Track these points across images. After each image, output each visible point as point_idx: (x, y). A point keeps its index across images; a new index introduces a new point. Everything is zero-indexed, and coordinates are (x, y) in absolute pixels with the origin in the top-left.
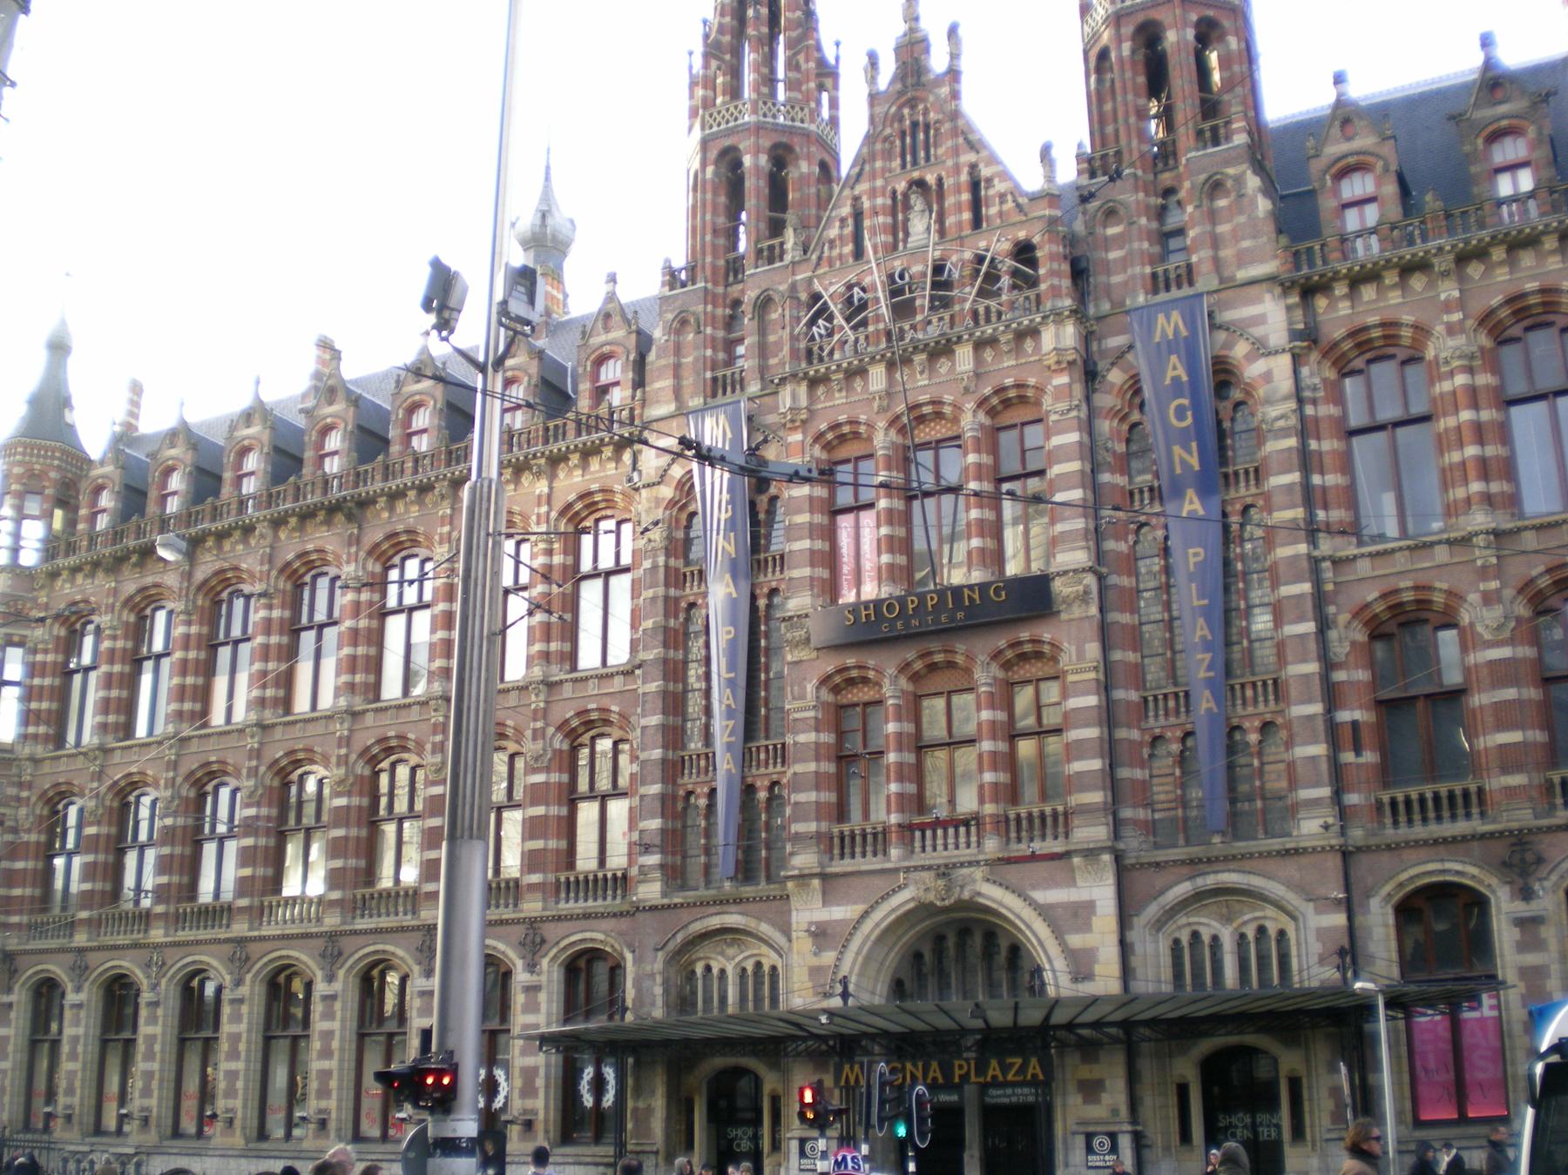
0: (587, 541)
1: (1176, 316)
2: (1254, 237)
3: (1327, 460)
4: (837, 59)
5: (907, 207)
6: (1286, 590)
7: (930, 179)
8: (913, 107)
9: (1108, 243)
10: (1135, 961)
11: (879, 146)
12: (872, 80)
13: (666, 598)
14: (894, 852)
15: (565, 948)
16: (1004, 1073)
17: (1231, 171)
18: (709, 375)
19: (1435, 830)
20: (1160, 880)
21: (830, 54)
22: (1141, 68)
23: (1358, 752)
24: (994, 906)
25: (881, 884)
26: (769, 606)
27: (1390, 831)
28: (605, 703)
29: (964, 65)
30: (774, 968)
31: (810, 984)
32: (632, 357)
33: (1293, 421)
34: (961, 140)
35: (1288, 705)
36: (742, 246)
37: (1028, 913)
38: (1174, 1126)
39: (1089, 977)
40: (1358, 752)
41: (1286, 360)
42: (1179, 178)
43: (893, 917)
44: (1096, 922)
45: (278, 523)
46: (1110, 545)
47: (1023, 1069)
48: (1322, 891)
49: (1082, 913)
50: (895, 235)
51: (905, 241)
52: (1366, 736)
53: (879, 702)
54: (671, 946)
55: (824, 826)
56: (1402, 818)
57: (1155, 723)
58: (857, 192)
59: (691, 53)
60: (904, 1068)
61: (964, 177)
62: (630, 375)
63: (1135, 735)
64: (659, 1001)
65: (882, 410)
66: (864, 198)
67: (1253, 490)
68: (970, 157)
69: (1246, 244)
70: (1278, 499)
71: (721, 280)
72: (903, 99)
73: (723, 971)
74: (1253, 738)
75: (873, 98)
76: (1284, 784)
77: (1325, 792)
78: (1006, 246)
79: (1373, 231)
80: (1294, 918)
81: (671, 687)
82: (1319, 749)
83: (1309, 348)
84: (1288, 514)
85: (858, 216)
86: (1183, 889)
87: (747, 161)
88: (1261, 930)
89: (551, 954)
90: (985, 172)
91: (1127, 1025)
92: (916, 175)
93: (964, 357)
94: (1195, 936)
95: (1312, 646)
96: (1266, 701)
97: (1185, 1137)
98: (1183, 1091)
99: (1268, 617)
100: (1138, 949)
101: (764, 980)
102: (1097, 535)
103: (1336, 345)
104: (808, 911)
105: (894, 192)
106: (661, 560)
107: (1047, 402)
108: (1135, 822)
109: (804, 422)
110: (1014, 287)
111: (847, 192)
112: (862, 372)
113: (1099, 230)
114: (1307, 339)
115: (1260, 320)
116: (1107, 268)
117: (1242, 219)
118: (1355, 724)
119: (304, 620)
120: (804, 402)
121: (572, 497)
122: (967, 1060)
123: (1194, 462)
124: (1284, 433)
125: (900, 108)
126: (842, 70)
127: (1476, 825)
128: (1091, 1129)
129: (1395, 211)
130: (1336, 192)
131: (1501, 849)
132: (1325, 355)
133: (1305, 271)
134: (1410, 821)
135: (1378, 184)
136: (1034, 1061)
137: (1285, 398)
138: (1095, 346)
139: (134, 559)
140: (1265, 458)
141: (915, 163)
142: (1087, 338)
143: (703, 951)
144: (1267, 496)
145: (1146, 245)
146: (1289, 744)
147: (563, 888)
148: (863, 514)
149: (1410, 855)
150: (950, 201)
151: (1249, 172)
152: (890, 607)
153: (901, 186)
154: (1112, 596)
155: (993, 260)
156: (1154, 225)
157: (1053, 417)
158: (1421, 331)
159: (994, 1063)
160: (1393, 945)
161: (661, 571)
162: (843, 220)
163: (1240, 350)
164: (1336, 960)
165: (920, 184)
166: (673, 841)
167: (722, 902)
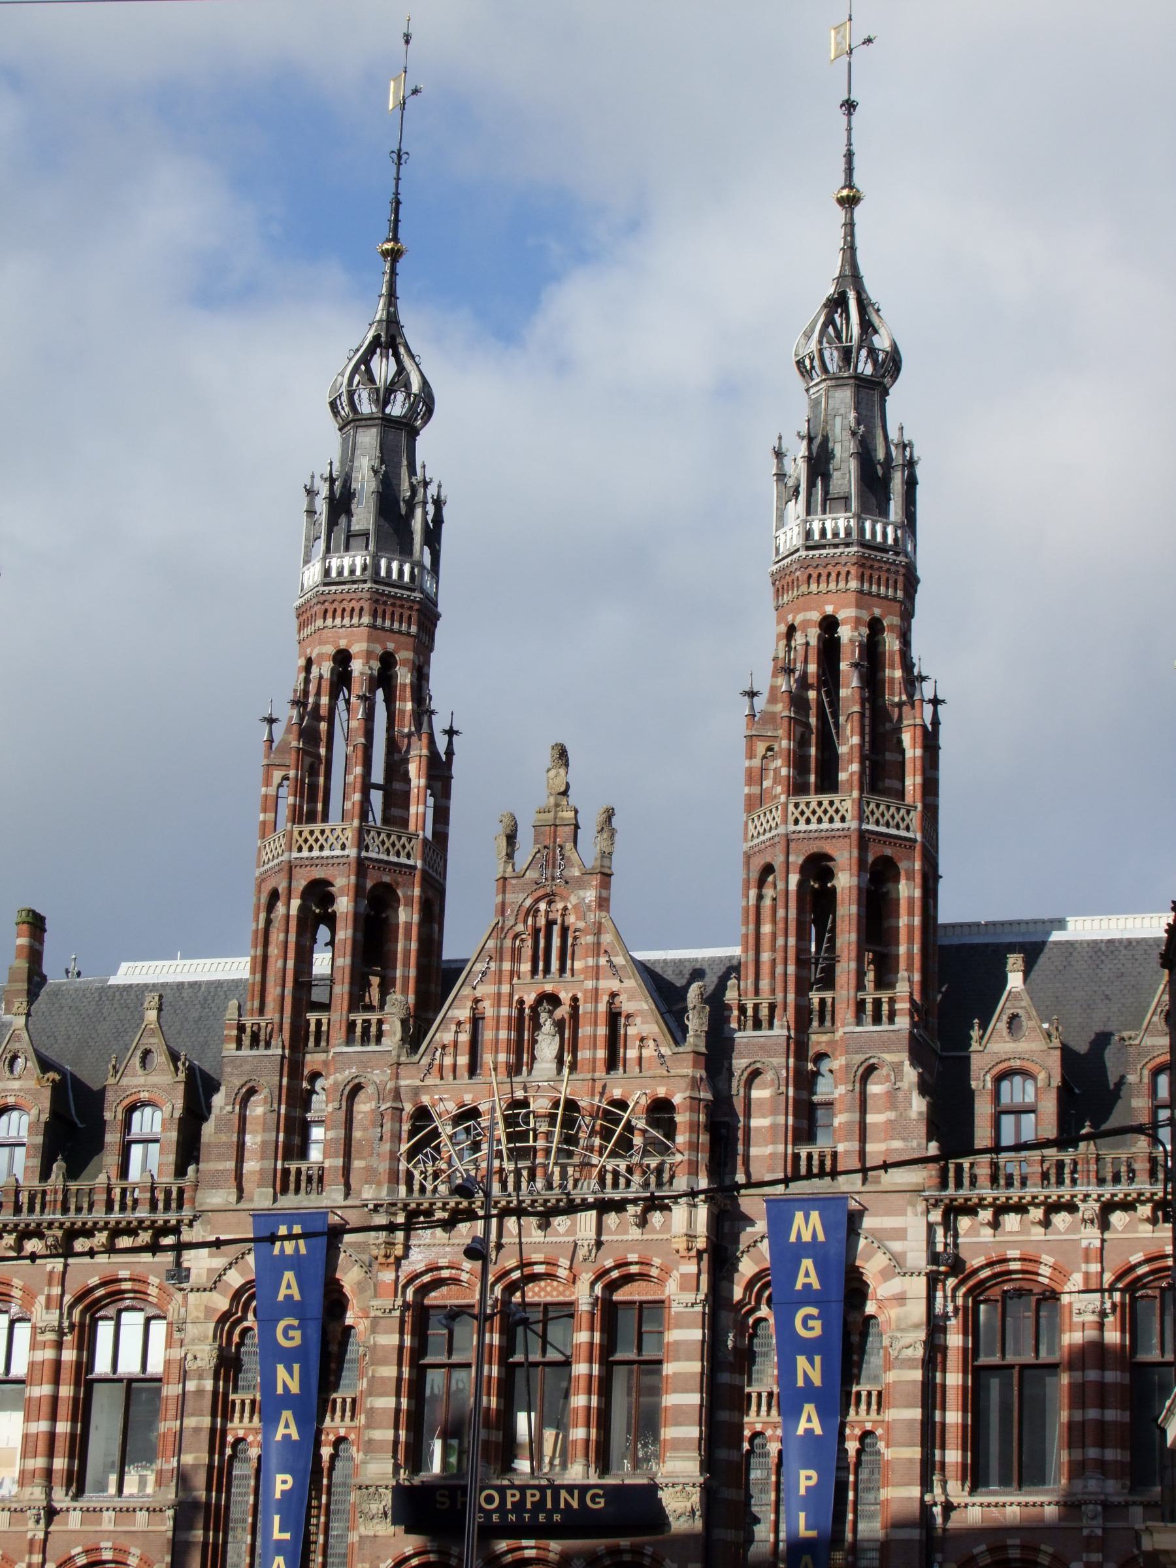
0: (105, 1331)
1: (815, 1216)
2: (904, 1139)
4: (450, 752)
5: (537, 1026)
7: (565, 996)
8: (550, 903)
17: (888, 1057)
21: (441, 743)
26: (334, 1457)
34: (603, 961)
41: (921, 1284)
58: (478, 993)
59: (271, 721)
61: (602, 1007)
62: (174, 1135)
66: (486, 1004)
68: (613, 985)
72: (541, 893)
78: (644, 1101)
85: (476, 1021)
92: (549, 988)
105: (521, 1002)
115: (900, 1234)
121: (94, 1281)
125: (537, 901)
137: (916, 1326)
138: (727, 1225)
144: (888, 1426)
151: (907, 1063)
153: (530, 999)
155: (629, 1121)
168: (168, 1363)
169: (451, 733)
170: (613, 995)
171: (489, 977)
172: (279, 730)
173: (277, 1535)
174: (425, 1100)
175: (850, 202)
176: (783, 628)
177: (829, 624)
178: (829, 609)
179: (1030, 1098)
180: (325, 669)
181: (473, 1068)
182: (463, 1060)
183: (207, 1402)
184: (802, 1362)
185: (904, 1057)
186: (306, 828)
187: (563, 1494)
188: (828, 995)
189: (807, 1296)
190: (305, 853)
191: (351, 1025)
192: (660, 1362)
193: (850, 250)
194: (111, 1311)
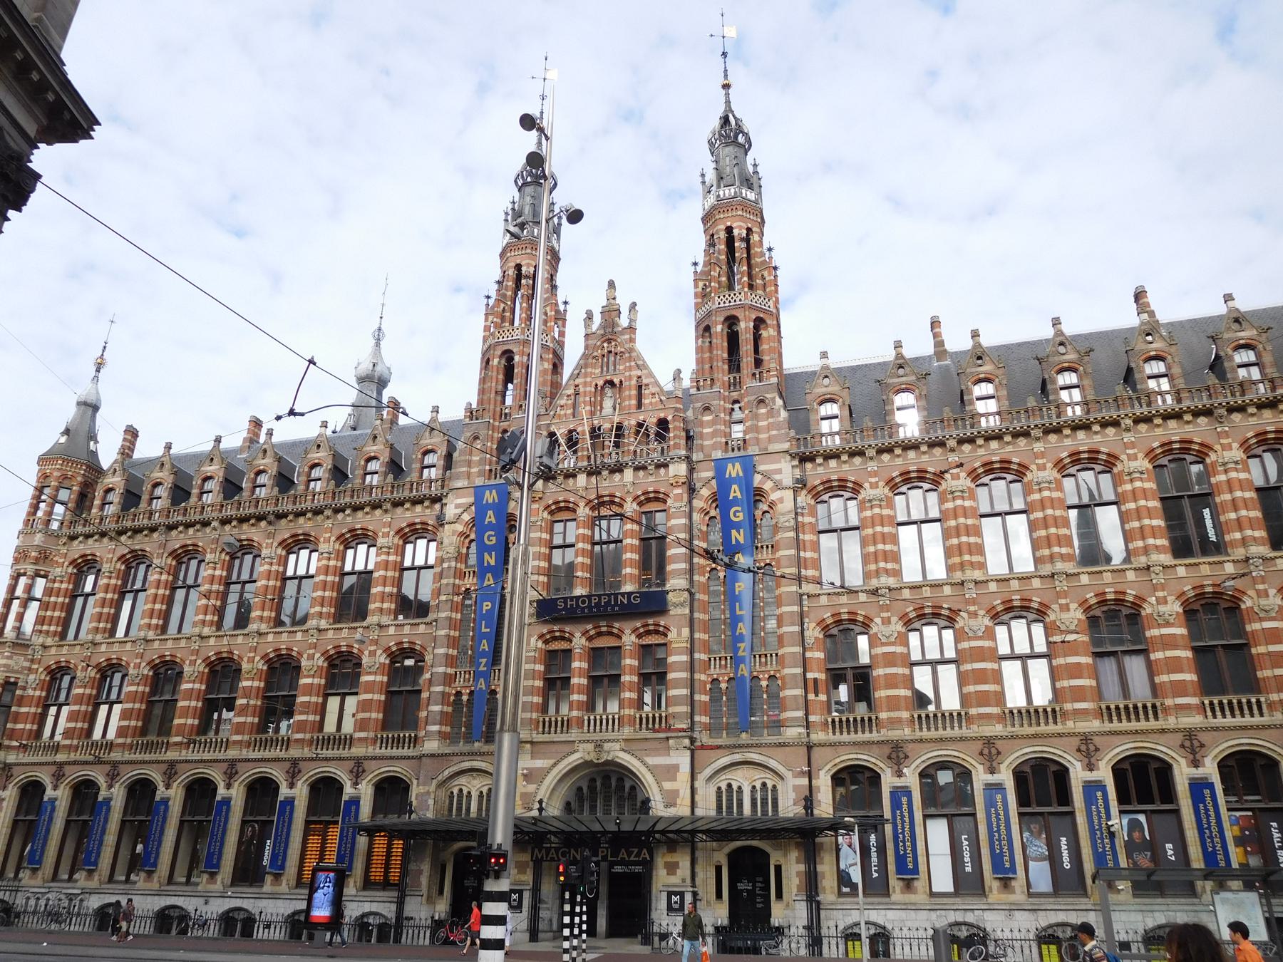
0: (409, 547)
1: (737, 465)
3: (808, 545)
5: (603, 394)
6: (785, 609)
7: (616, 381)
9: (702, 424)
10: (697, 798)
12: (587, 326)
14: (574, 730)
15: (377, 775)
16: (629, 857)
17: (768, 396)
18: (487, 468)
19: (853, 737)
21: (562, 307)
22: (725, 338)
23: (817, 695)
24: (626, 764)
25: (566, 748)
33: (792, 523)
34: (633, 363)
36: (509, 400)
39: (674, 805)
40: (817, 695)
42: (742, 396)
43: (570, 767)
44: (679, 776)
45: (225, 522)
47: (638, 855)
49: (672, 771)
51: (601, 411)
52: (822, 687)
53: (570, 651)
55: (534, 715)
56: (837, 730)
58: (577, 381)
60: (569, 852)
61: (634, 382)
62: (442, 462)
63: (703, 677)
67: (770, 556)
68: (639, 373)
70: (783, 562)
71: (498, 418)
74: (764, 683)
75: (587, 336)
77: (800, 714)
78: (655, 420)
79: (837, 433)
82: (799, 692)
83: (802, 488)
87: (517, 358)
88: (764, 784)
89: (369, 778)
90: (645, 381)
91: (693, 833)
92: (608, 378)
93: (628, 474)
94: (729, 786)
96: (771, 664)
97: (719, 895)
98: (718, 870)
99: (774, 622)
102: (691, 571)
106: (453, 564)
107: (670, 502)
109: (540, 498)
111: (572, 382)
112: (574, 476)
115: (779, 471)
116: (702, 436)
118: (815, 680)
119: (234, 578)
122: (607, 848)
124: (788, 529)
127: (874, 736)
128: (670, 889)
129: (847, 426)
133: (802, 449)
134: (841, 733)
139: (129, 534)
142: (691, 470)
144: (778, 561)
146: (783, 688)
147: (379, 741)
148: (567, 550)
149: (840, 749)
153: (601, 383)
154: (696, 604)
157: (673, 510)
159: (623, 850)
163: (767, 486)
164: (803, 803)
165: (611, 383)
167: (473, 755)
169: (566, 303)
170: (639, 377)
172: (491, 302)
173: (484, 630)
175: (726, 87)
177: (729, 230)
178: (729, 224)
180: (511, 272)
183: (452, 571)
184: (734, 532)
187: (620, 597)
188: (737, 376)
193: (728, 102)
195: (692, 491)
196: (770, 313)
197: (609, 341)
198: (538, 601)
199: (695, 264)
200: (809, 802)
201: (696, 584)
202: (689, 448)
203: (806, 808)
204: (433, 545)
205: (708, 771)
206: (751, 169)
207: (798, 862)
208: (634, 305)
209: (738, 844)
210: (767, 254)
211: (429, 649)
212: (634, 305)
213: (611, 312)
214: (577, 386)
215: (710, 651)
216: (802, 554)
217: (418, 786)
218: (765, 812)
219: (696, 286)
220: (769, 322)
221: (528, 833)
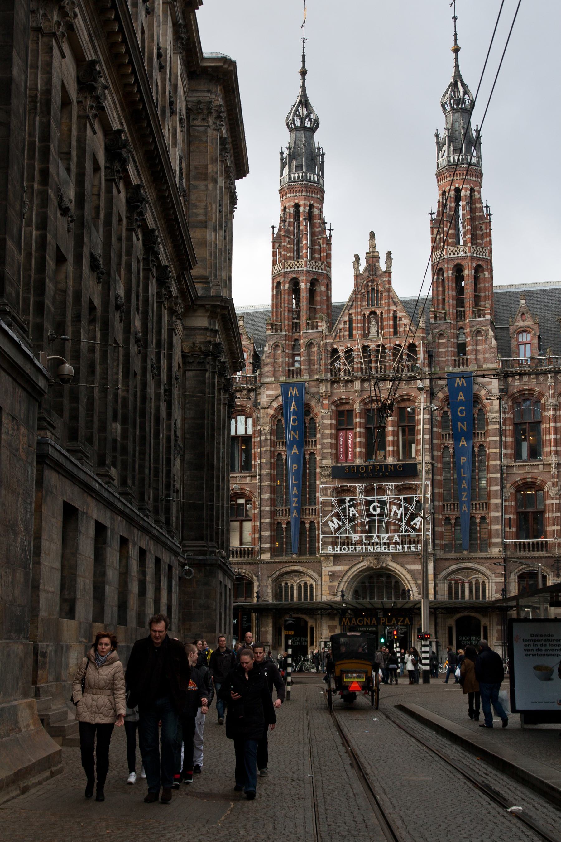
0: (233, 422)
3: (507, 433)
4: (330, 236)
5: (369, 322)
6: (492, 475)
7: (378, 312)
9: (440, 345)
10: (437, 589)
11: (359, 296)
12: (357, 269)
13: (271, 451)
17: (484, 328)
18: (287, 368)
20: (447, 563)
21: (328, 233)
23: (510, 528)
27: (518, 553)
28: (244, 486)
29: (393, 269)
30: (311, 585)
31: (328, 592)
32: (252, 353)
34: (391, 300)
35: (490, 512)
37: (404, 572)
38: (447, 640)
40: (510, 528)
46: (435, 453)
47: (403, 621)
48: (497, 571)
50: (364, 330)
52: (513, 523)
54: (274, 576)
56: (522, 549)
57: (447, 513)
59: (273, 227)
61: (391, 315)
63: (440, 516)
64: (270, 595)
65: (358, 396)
66: (353, 315)
67: (483, 440)
69: (487, 355)
70: (491, 445)
73: (292, 585)
74: (478, 521)
76: (487, 536)
80: (488, 578)
81: (273, 484)
84: (494, 451)
85: (351, 321)
86: (454, 567)
92: (373, 310)
95: (499, 494)
98: (450, 629)
99: (485, 482)
100: (439, 585)
101: (306, 589)
102: (432, 450)
103: (513, 394)
104: (328, 568)
105: (364, 314)
106: (269, 437)
108: (439, 544)
110: (409, 361)
111: (347, 311)
112: (352, 381)
113: (437, 341)
114: (505, 392)
117: (486, 346)
118: (510, 519)
120: (329, 390)
123: (465, 428)
124: (495, 423)
125: (368, 282)
126: (333, 241)
130: (517, 339)
131: (551, 561)
132: (509, 397)
134: (525, 551)
135: (532, 339)
136: (407, 619)
137: (496, 412)
140: (489, 430)
141: (372, 305)
143: (286, 577)
144: (488, 443)
145: (453, 349)
146: (490, 524)
150: (386, 323)
152: (362, 469)
153: (367, 313)
154: (435, 470)
156: (456, 341)
158: (541, 394)
160: (517, 588)
161: (269, 441)
162: (345, 322)
163: (483, 393)
165: (374, 313)
166: (272, 539)
167: (295, 563)
168: (254, 431)
169: (330, 230)
170: (395, 311)
171: (353, 307)
172: (276, 231)
174: (335, 346)
176: (441, 192)
179: (529, 339)
180: (292, 210)
181: (351, 336)
182: (347, 333)
184: (460, 424)
185: (489, 327)
186: (289, 262)
188: (462, 309)
189: (461, 403)
190: (289, 269)
191: (308, 324)
192: (415, 426)
194: (234, 416)
195: (432, 394)
196: (486, 260)
197: (372, 281)
198: (333, 468)
199: (432, 214)
200: (504, 591)
201: (435, 458)
202: (430, 365)
203: (502, 595)
204: (250, 421)
205: (444, 573)
206: (474, 134)
207: (497, 625)
208: (389, 253)
209: (462, 615)
210: (485, 209)
211: (257, 494)
212: (389, 253)
213: (373, 258)
214: (350, 314)
215: (444, 500)
216: (503, 439)
217: (258, 580)
218: (477, 597)
219: (432, 233)
220: (485, 267)
221: (336, 609)
